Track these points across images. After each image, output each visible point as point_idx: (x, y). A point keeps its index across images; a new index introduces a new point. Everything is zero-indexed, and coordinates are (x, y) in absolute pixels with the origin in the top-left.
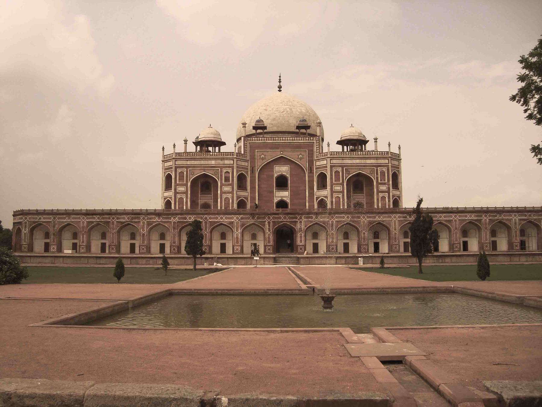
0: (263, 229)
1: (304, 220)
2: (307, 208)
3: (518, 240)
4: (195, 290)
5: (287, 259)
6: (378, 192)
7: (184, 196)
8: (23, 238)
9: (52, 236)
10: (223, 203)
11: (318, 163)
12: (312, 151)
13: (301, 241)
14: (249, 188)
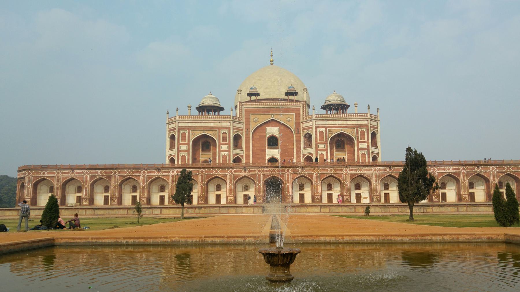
0: (254, 182)
6: (359, 149)
8: (26, 192)
11: (304, 125)
12: (299, 114)
13: (288, 192)
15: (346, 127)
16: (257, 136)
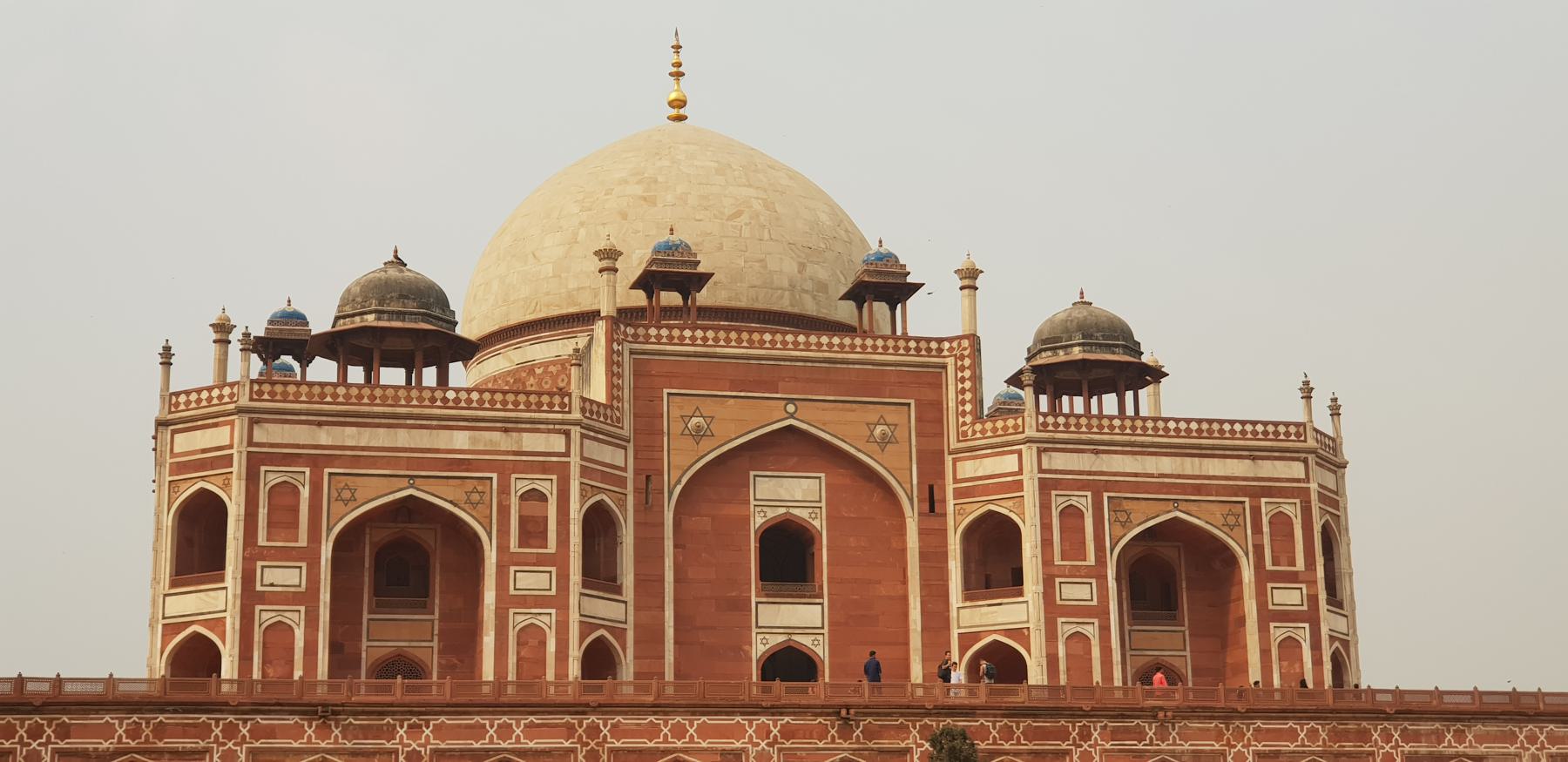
6: (1268, 616)
7: (295, 618)
10: (512, 659)
11: (968, 469)
14: (628, 579)
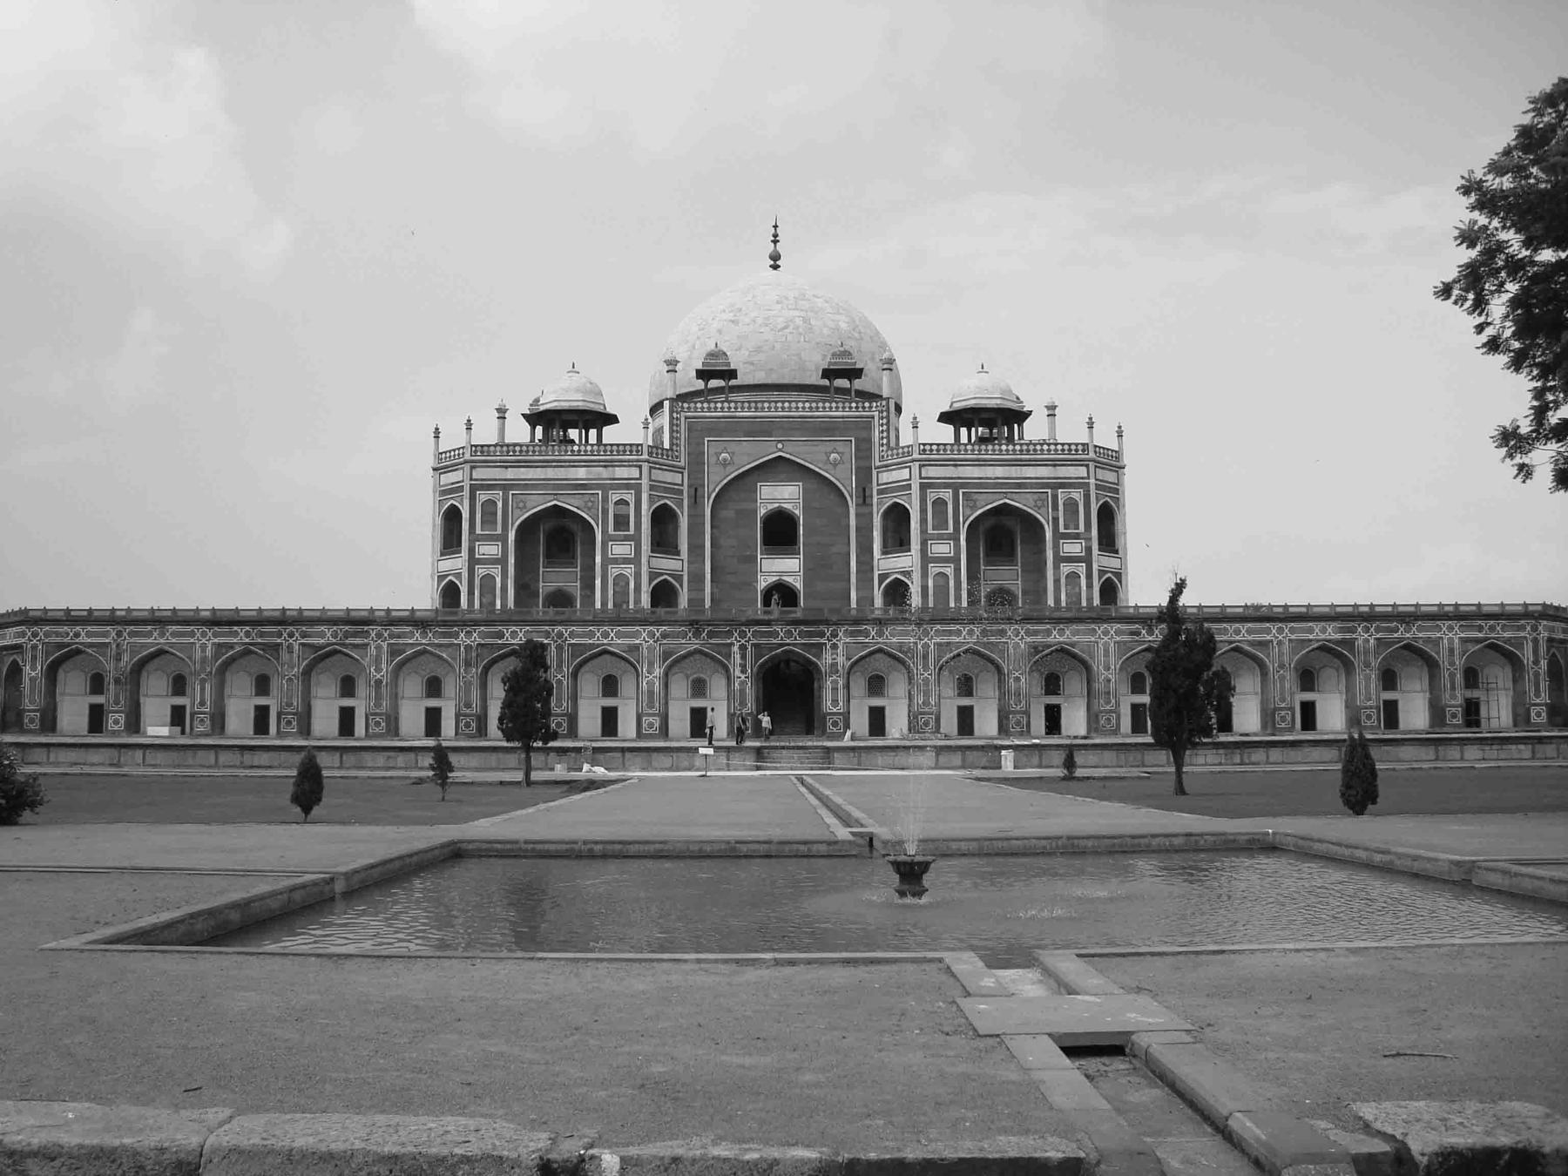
0: (727, 670)
1: (843, 639)
2: (854, 605)
3: (1459, 701)
4: (526, 842)
5: (796, 754)
6: (1059, 559)
7: (496, 571)
8: (27, 691)
9: (112, 687)
10: (611, 592)
11: (886, 477)
12: (869, 441)
13: (835, 702)
14: (684, 546)
15: (1019, 486)
16: (728, 514)
